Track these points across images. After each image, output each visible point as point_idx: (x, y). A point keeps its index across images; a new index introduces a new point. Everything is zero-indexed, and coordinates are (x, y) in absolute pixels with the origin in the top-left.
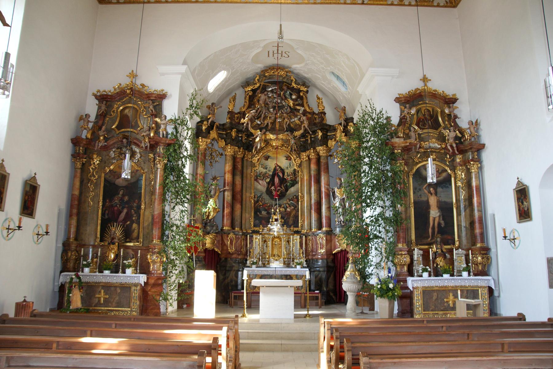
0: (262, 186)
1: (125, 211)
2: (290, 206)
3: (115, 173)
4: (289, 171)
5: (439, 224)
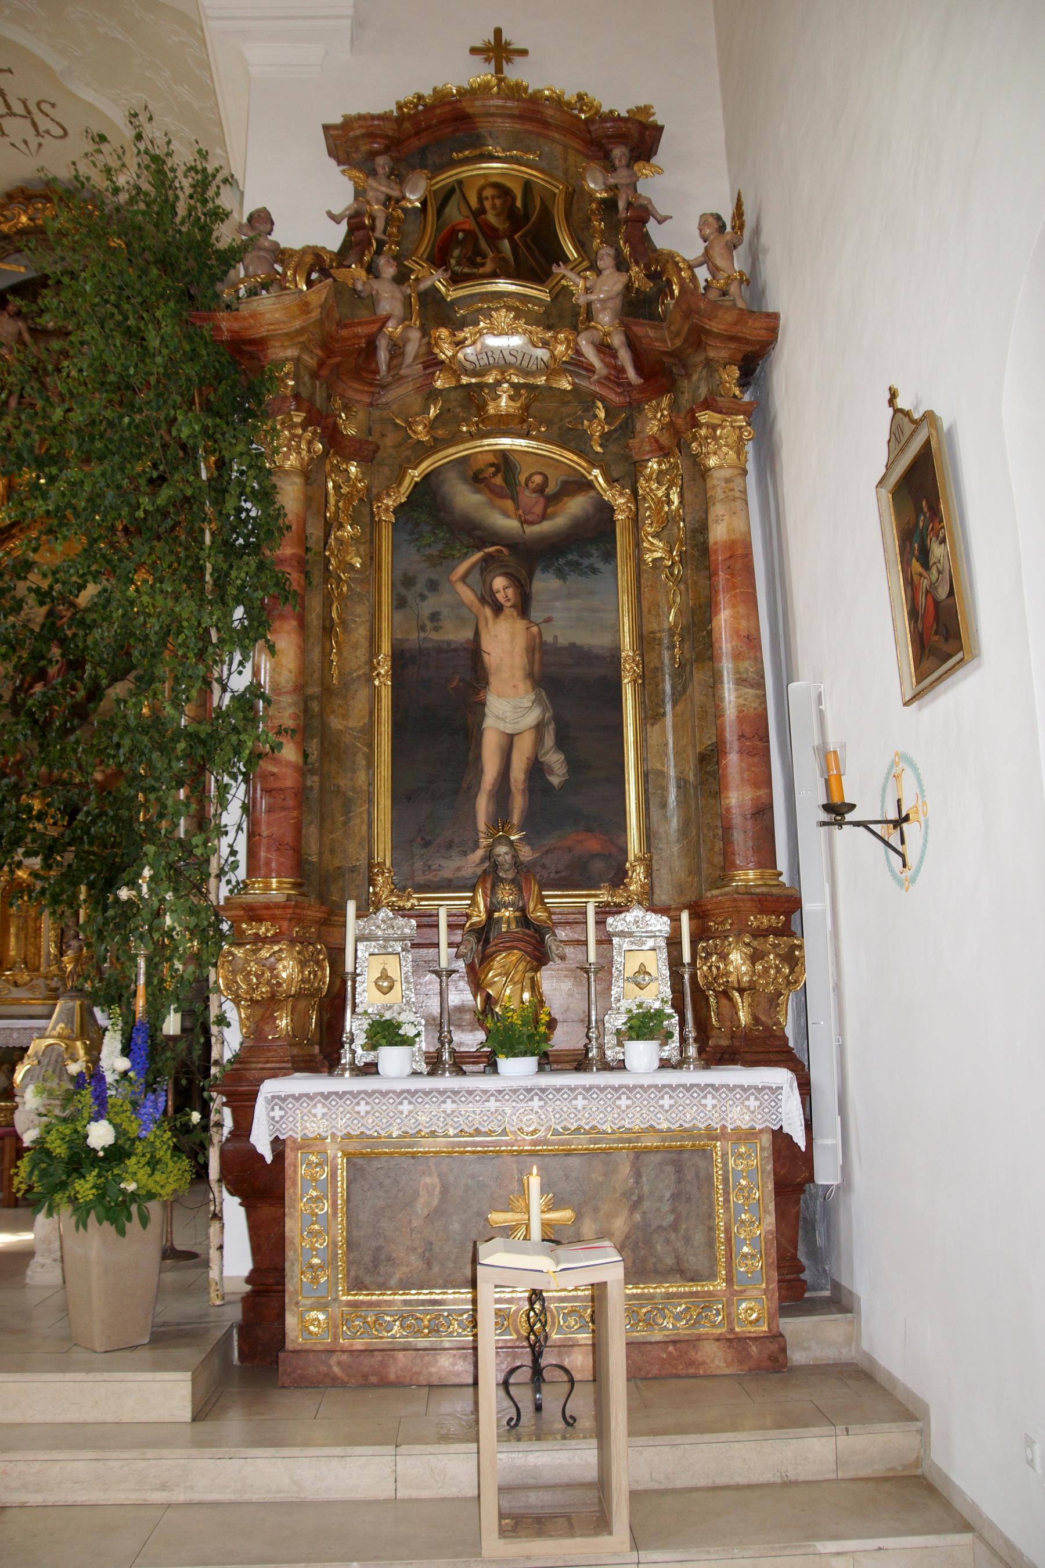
5: (536, 769)
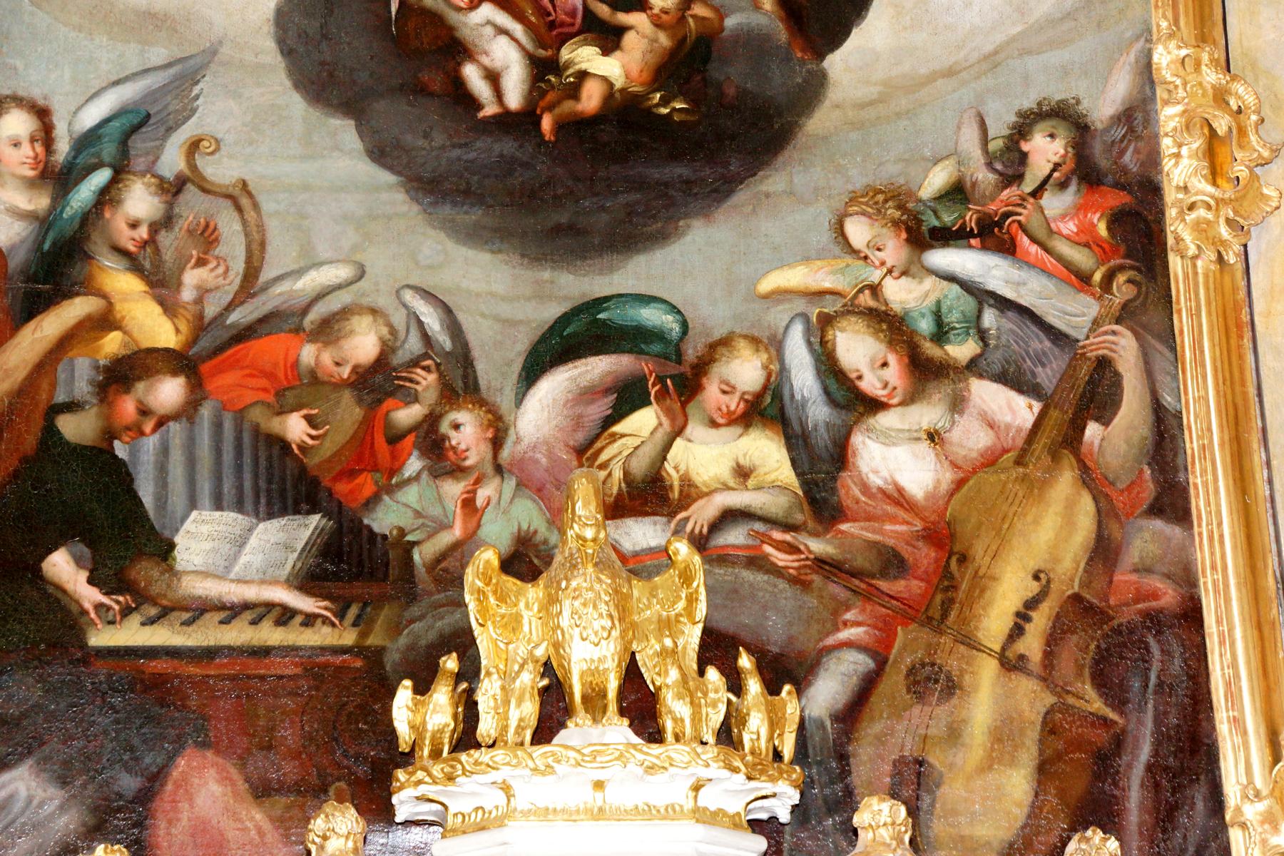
2: (925, 372)
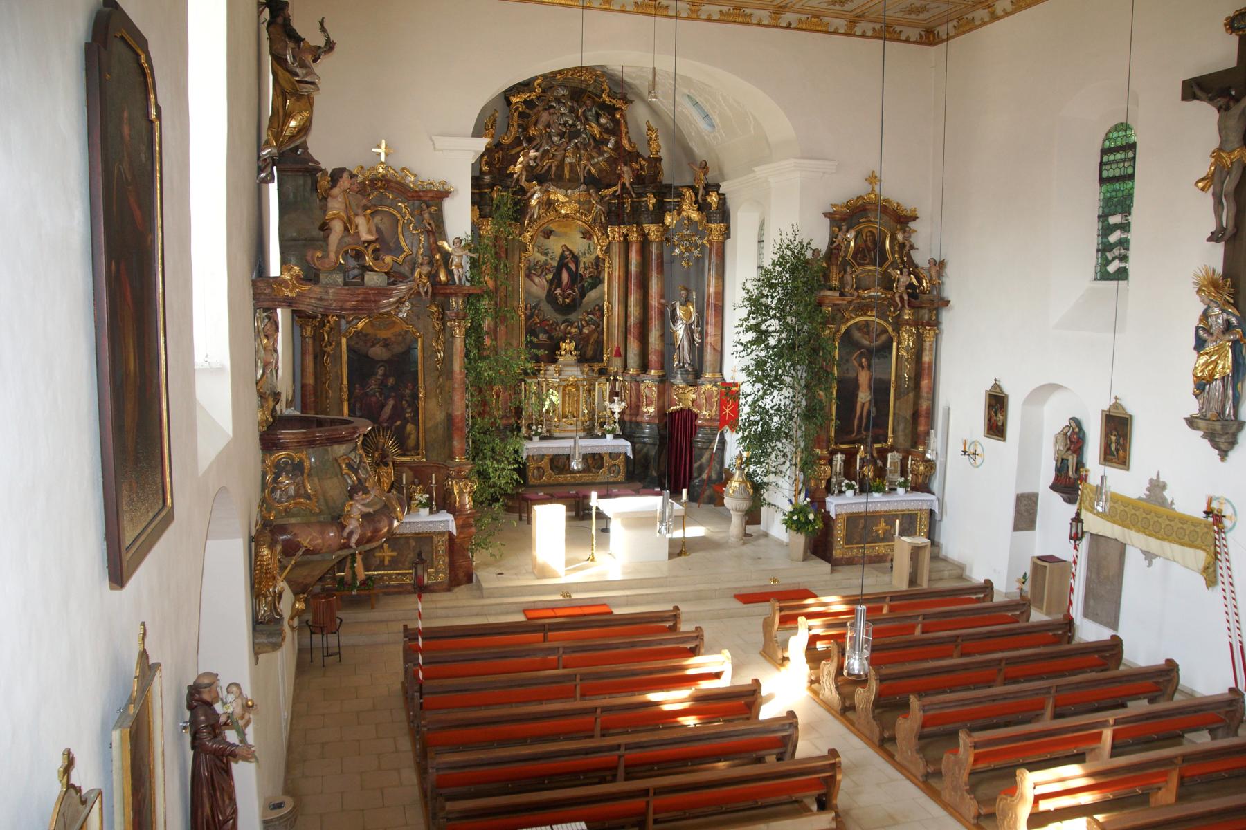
0: (539, 287)
1: (391, 403)
3: (366, 335)
4: (587, 260)
5: (869, 412)
